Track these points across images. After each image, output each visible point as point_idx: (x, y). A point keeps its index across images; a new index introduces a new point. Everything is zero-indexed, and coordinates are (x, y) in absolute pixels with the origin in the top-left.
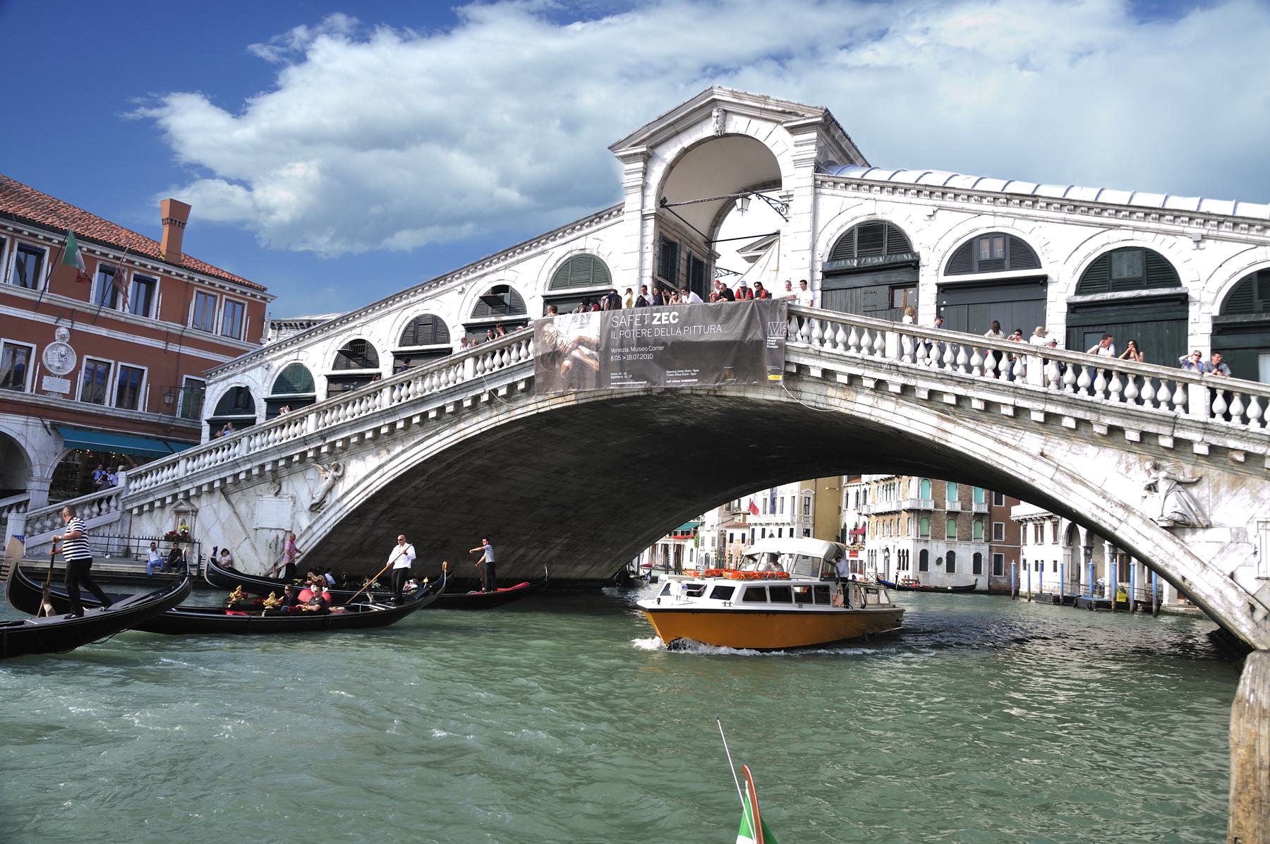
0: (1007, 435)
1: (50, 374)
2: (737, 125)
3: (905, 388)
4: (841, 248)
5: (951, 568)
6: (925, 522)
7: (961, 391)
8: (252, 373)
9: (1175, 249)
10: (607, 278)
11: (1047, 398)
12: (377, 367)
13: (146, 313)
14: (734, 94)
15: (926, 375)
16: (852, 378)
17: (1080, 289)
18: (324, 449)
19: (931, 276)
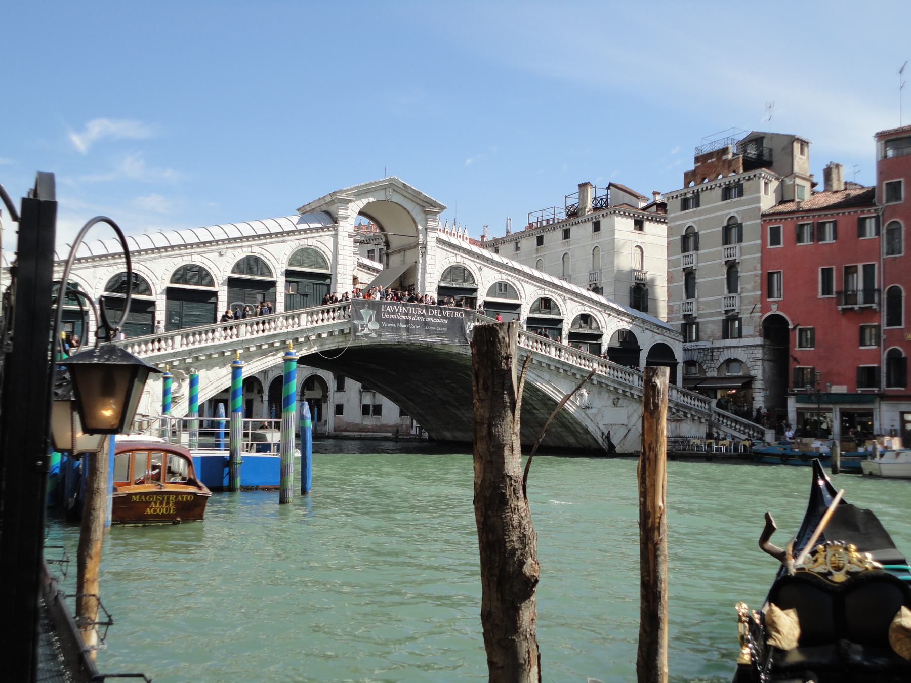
0: (539, 373)
2: (397, 198)
11: (559, 361)
12: (150, 294)
18: (189, 361)
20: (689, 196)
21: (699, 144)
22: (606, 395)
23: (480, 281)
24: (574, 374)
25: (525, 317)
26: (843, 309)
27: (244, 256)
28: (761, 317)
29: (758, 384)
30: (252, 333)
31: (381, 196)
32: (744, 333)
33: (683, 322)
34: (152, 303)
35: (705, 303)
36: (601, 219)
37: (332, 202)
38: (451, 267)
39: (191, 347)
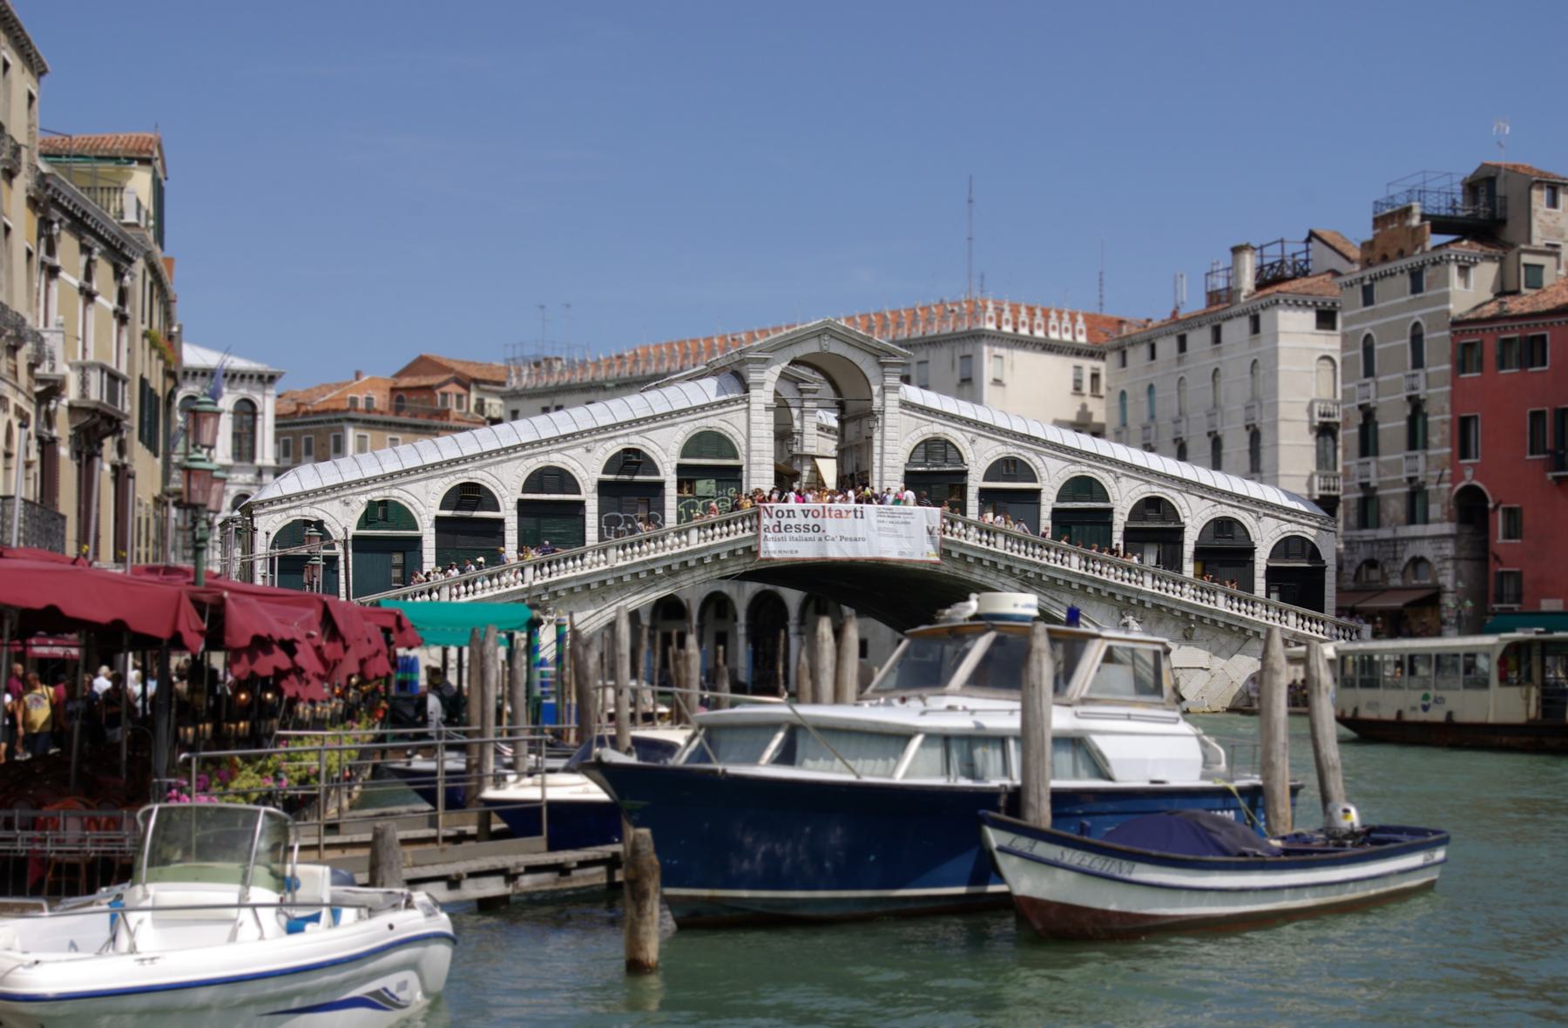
7: (1037, 570)
8: (326, 506)
9: (1106, 480)
11: (1083, 576)
12: (498, 510)
17: (1060, 498)
20: (1367, 282)
21: (1381, 195)
22: (1171, 625)
23: (971, 456)
24: (1112, 595)
25: (1049, 509)
26: (1555, 478)
27: (619, 449)
28: (1451, 489)
29: (1449, 601)
30: (624, 558)
31: (811, 347)
32: (1431, 516)
33: (1360, 495)
34: (501, 522)
35: (1386, 464)
36: (1261, 312)
37: (743, 362)
38: (925, 442)
39: (546, 580)
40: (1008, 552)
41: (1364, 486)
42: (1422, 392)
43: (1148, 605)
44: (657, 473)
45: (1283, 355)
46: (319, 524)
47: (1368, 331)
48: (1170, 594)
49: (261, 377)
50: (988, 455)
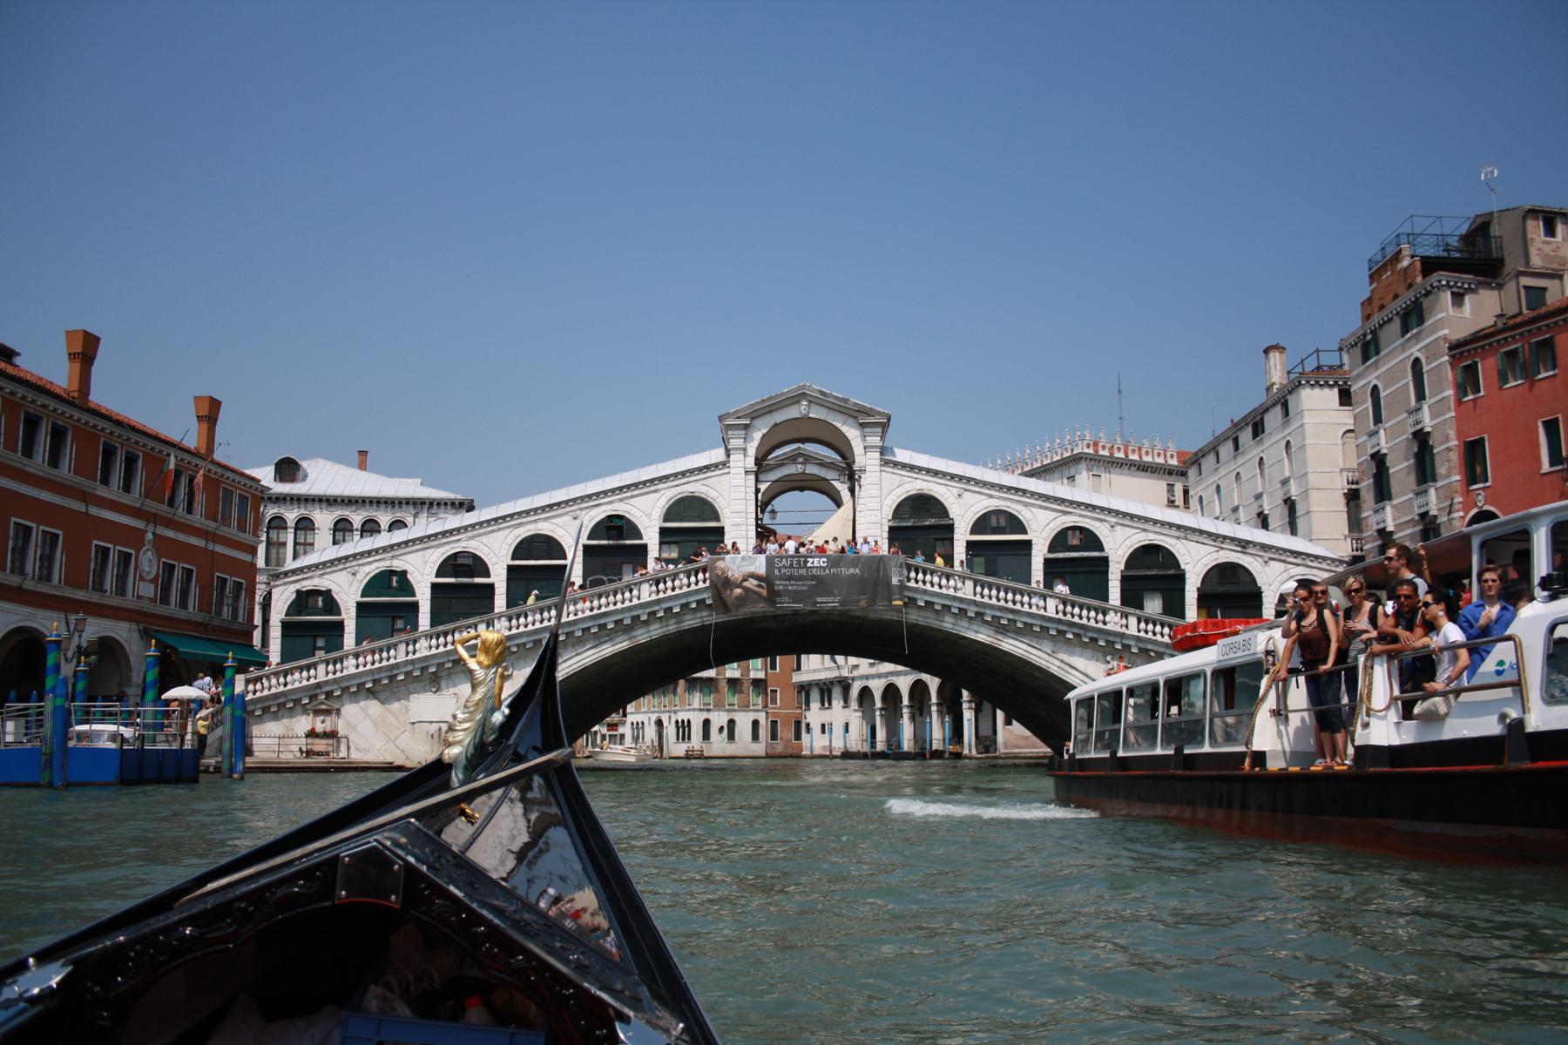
1: (142, 579)
3: (977, 613)
4: (898, 512)
5: (731, 737)
6: (706, 690)
7: (1011, 616)
9: (1101, 530)
10: (717, 518)
11: (1059, 621)
12: (488, 576)
13: (190, 510)
14: (822, 393)
15: (992, 607)
16: (946, 608)
17: (1051, 549)
19: (962, 536)
34: (491, 587)
40: (978, 598)
41: (1382, 532)
42: (1428, 423)
43: (1134, 650)
44: (639, 535)
45: (1308, 429)
46: (327, 595)
47: (1375, 382)
48: (1158, 637)
49: (453, 504)
50: (975, 509)
